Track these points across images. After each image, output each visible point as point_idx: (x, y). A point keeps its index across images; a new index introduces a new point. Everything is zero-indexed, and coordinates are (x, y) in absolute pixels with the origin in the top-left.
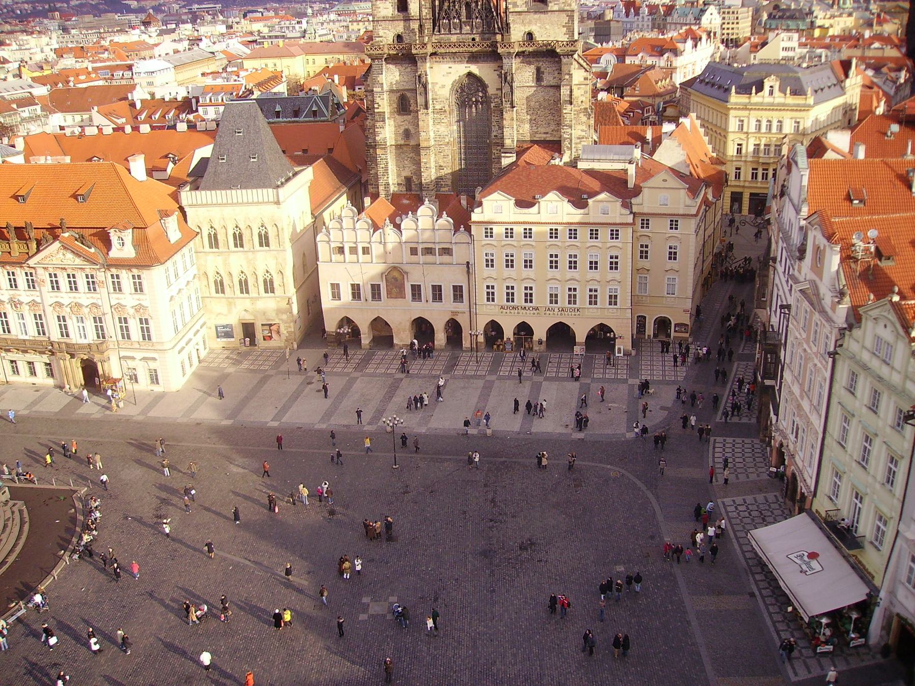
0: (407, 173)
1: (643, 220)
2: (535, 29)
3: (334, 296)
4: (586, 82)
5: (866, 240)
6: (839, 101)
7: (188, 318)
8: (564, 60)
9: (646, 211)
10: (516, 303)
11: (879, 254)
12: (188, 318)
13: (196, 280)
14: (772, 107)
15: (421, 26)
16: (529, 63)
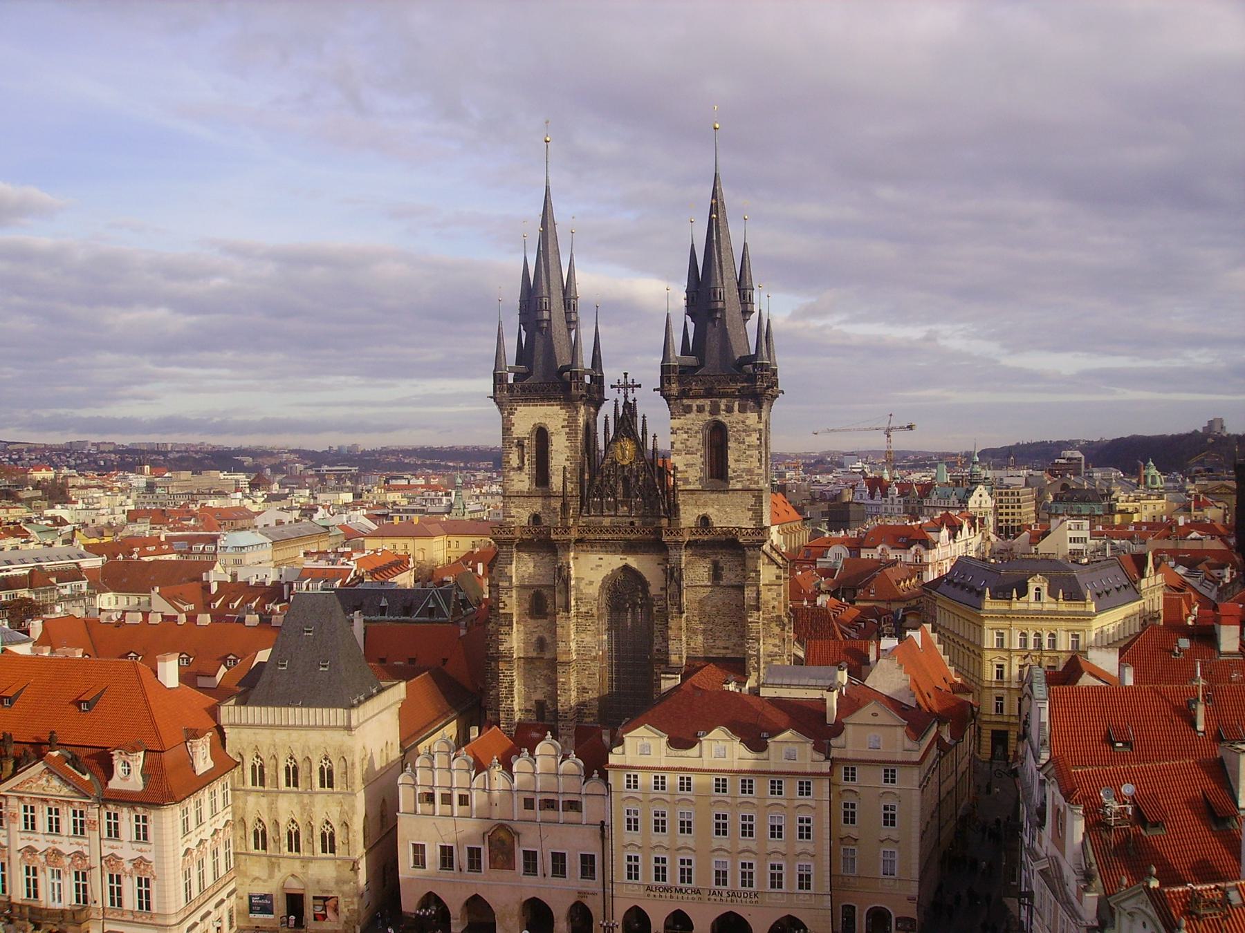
0: (539, 696)
1: (846, 769)
2: (711, 511)
3: (416, 862)
4: (778, 582)
5: (1119, 797)
6: (1134, 607)
7: (209, 881)
8: (749, 553)
9: (850, 755)
10: (668, 882)
11: (1140, 818)
12: (209, 881)
13: (228, 829)
14: (1039, 615)
15: (564, 505)
16: (704, 556)
